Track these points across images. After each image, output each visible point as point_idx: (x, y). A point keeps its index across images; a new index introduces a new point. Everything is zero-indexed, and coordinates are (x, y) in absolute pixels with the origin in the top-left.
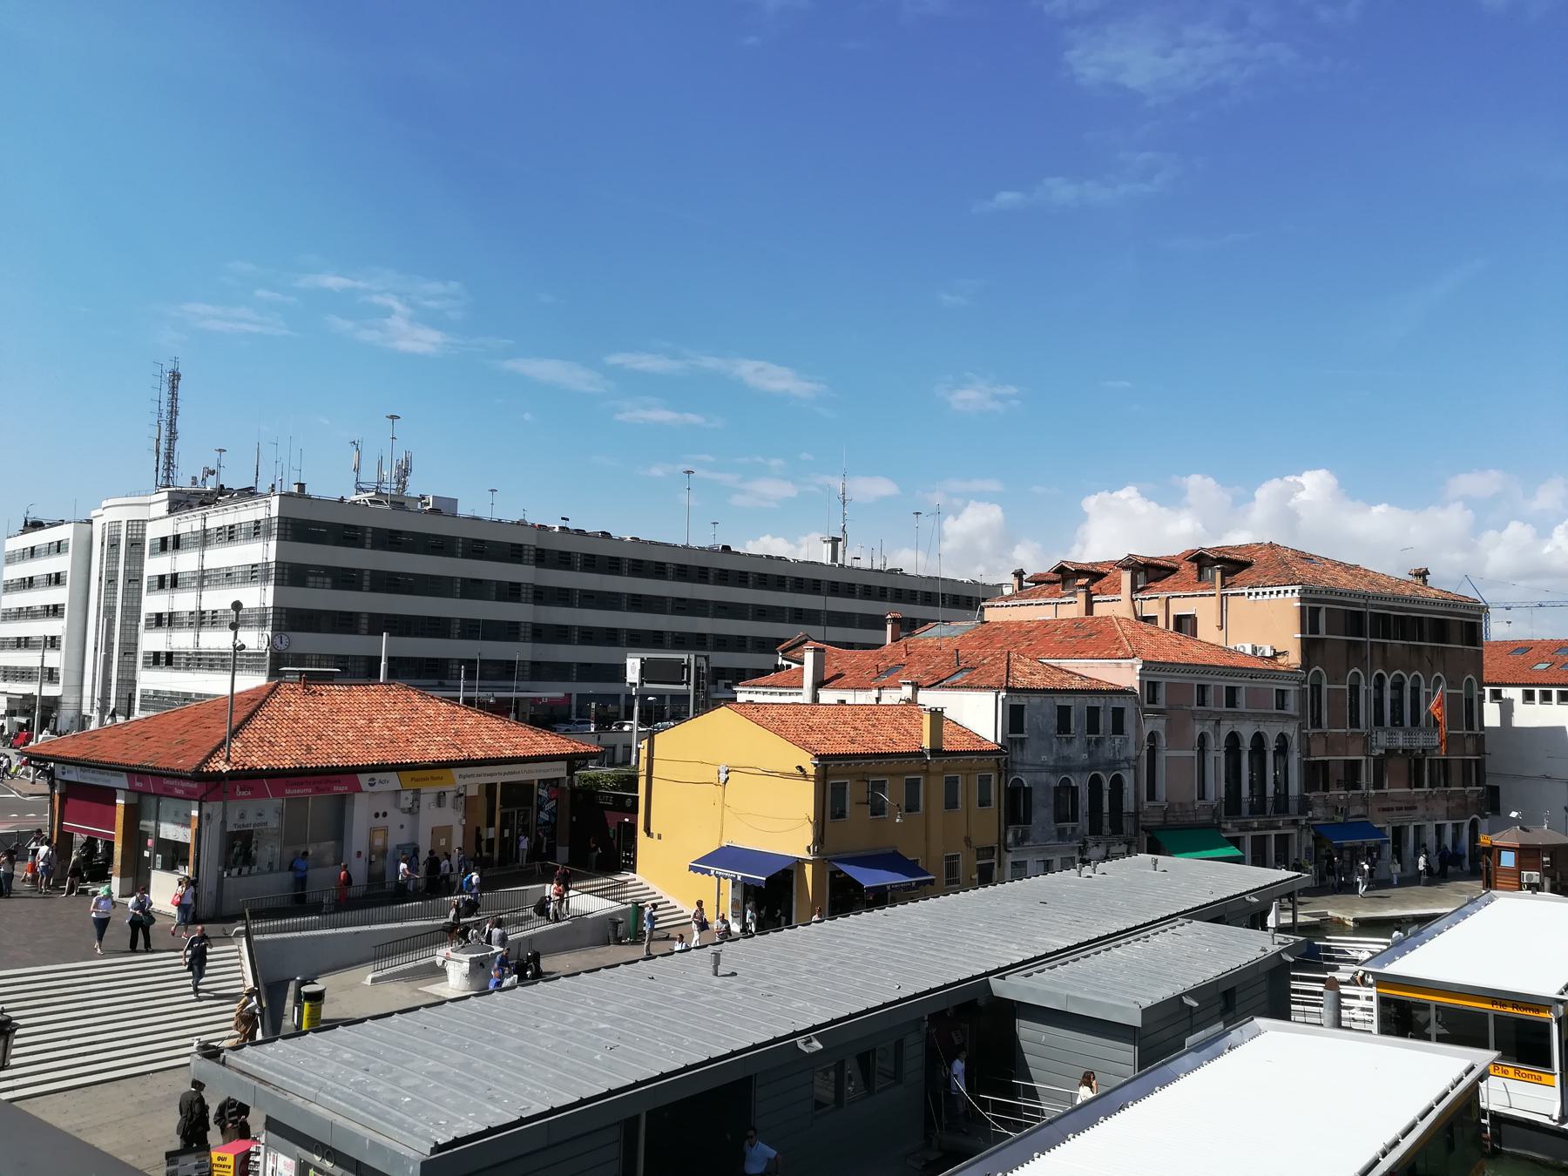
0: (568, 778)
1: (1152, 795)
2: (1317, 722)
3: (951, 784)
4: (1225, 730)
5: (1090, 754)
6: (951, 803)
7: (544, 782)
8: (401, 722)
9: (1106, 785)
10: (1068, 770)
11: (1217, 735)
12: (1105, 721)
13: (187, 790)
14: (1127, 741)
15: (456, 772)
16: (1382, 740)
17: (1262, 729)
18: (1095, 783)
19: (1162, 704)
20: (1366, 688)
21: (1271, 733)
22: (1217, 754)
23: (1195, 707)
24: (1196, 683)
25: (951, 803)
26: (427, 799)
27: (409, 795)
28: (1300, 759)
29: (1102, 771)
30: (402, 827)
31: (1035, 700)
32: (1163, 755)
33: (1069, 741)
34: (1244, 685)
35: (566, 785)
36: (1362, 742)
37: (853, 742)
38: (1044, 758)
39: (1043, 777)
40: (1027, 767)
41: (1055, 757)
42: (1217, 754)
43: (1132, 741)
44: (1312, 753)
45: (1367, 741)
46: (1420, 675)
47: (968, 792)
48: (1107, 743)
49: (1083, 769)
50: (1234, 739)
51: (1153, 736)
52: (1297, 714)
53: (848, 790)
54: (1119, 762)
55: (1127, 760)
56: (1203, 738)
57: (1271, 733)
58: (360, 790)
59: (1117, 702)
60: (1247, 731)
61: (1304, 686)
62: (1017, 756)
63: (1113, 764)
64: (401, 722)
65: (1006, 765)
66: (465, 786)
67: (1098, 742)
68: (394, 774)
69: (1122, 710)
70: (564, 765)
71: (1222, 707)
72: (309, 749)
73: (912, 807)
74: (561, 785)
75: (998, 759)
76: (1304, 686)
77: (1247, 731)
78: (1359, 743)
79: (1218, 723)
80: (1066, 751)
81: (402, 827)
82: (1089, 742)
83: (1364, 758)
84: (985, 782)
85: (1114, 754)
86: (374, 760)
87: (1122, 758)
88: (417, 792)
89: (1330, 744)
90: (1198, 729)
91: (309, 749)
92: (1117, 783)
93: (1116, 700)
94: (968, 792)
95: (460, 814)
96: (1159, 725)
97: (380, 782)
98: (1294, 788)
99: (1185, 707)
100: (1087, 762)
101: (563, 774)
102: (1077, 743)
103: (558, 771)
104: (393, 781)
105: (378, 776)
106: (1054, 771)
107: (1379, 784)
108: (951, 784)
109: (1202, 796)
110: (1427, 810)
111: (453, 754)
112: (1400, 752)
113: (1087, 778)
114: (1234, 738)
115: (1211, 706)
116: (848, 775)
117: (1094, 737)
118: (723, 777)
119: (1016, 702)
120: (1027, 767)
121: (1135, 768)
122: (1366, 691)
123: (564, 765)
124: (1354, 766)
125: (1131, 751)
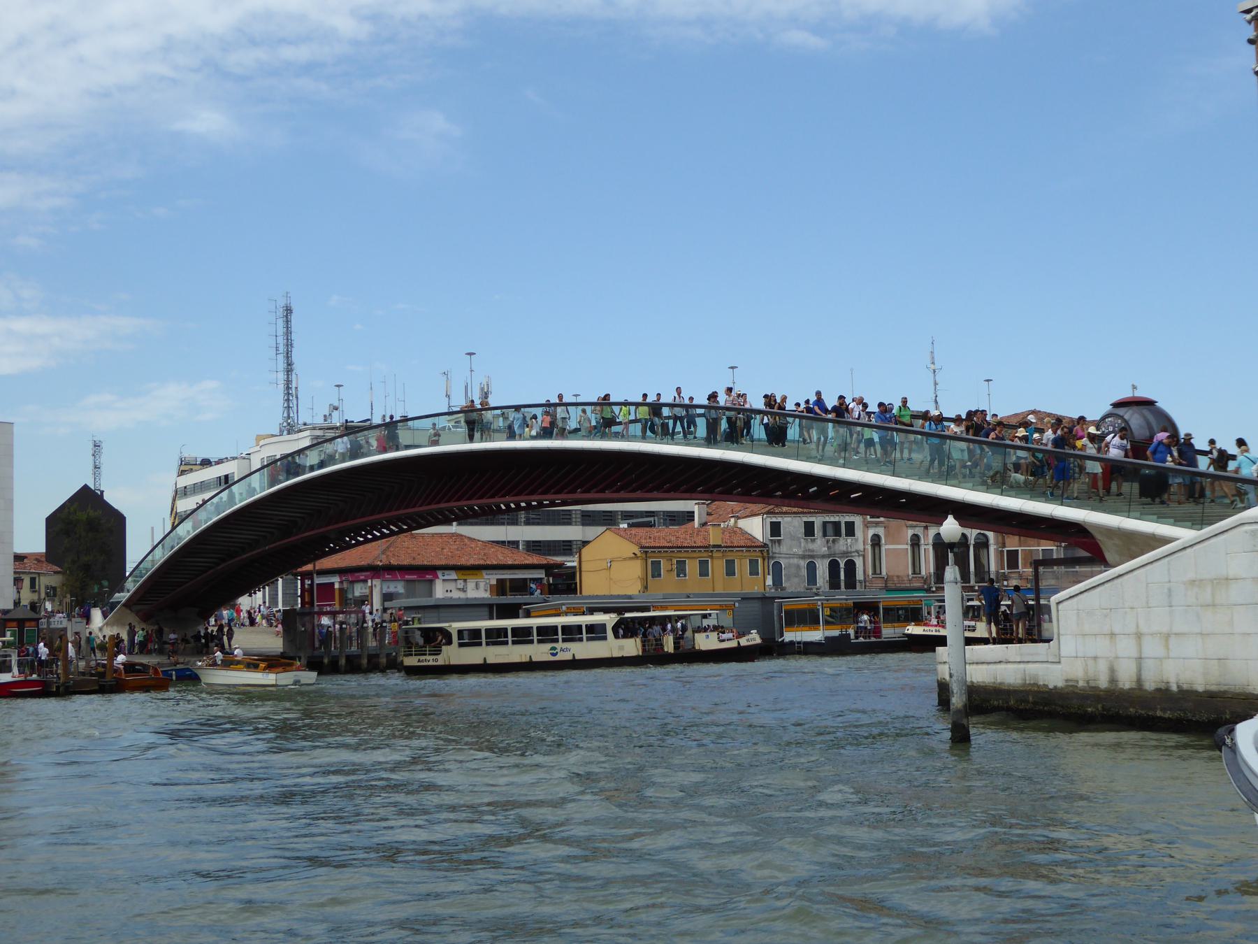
5: (829, 548)
7: (534, 580)
8: (457, 549)
9: (842, 565)
11: (926, 536)
13: (365, 576)
14: (857, 540)
15: (484, 572)
18: (834, 566)
28: (996, 550)
33: (813, 541)
39: (796, 561)
42: (926, 547)
44: (1007, 545)
49: (823, 557)
54: (851, 552)
55: (857, 551)
58: (437, 577)
62: (776, 549)
63: (845, 554)
64: (457, 549)
65: (768, 554)
69: (853, 523)
70: (543, 571)
72: (414, 559)
80: (811, 546)
82: (828, 542)
83: (1055, 548)
85: (847, 548)
86: (443, 563)
87: (853, 550)
91: (414, 559)
92: (851, 566)
101: (543, 576)
104: (453, 575)
105: (446, 572)
106: (803, 557)
111: (481, 562)
113: (827, 562)
116: (663, 557)
119: (774, 520)
121: (864, 556)
123: (543, 571)
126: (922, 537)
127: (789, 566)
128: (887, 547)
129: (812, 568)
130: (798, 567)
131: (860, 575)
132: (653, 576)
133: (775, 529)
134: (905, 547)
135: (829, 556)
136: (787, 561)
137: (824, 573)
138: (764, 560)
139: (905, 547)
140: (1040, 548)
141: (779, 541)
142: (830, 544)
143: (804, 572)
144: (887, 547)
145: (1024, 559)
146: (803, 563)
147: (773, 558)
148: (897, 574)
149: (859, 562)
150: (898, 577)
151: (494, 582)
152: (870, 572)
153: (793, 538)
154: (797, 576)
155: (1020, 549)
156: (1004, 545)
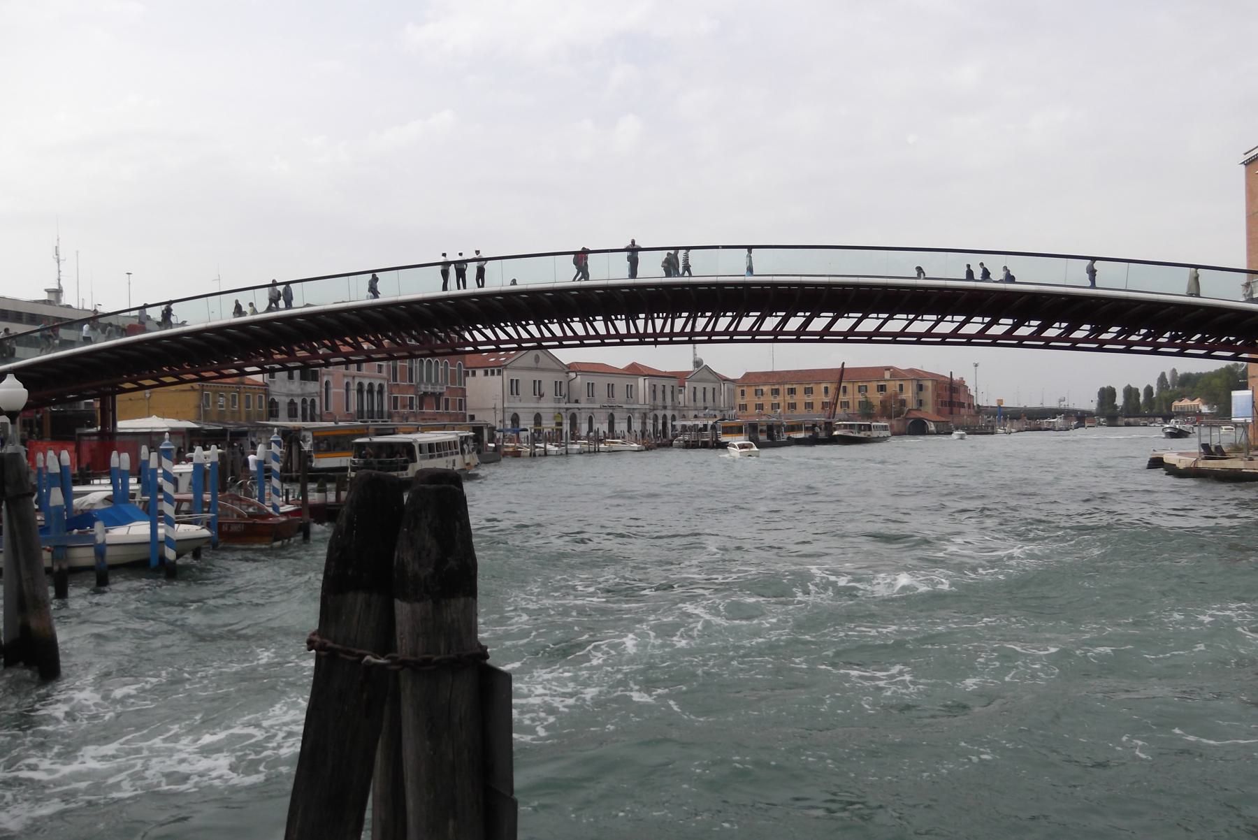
1: (327, 409)
2: (395, 380)
4: (357, 381)
5: (302, 389)
11: (354, 383)
18: (304, 401)
21: (376, 383)
45: (416, 388)
50: (360, 384)
51: (327, 383)
55: (317, 393)
56: (348, 384)
57: (376, 383)
60: (366, 382)
77: (366, 382)
79: (354, 377)
90: (346, 380)
92: (313, 401)
98: (386, 408)
106: (287, 395)
114: (360, 384)
135: (302, 395)
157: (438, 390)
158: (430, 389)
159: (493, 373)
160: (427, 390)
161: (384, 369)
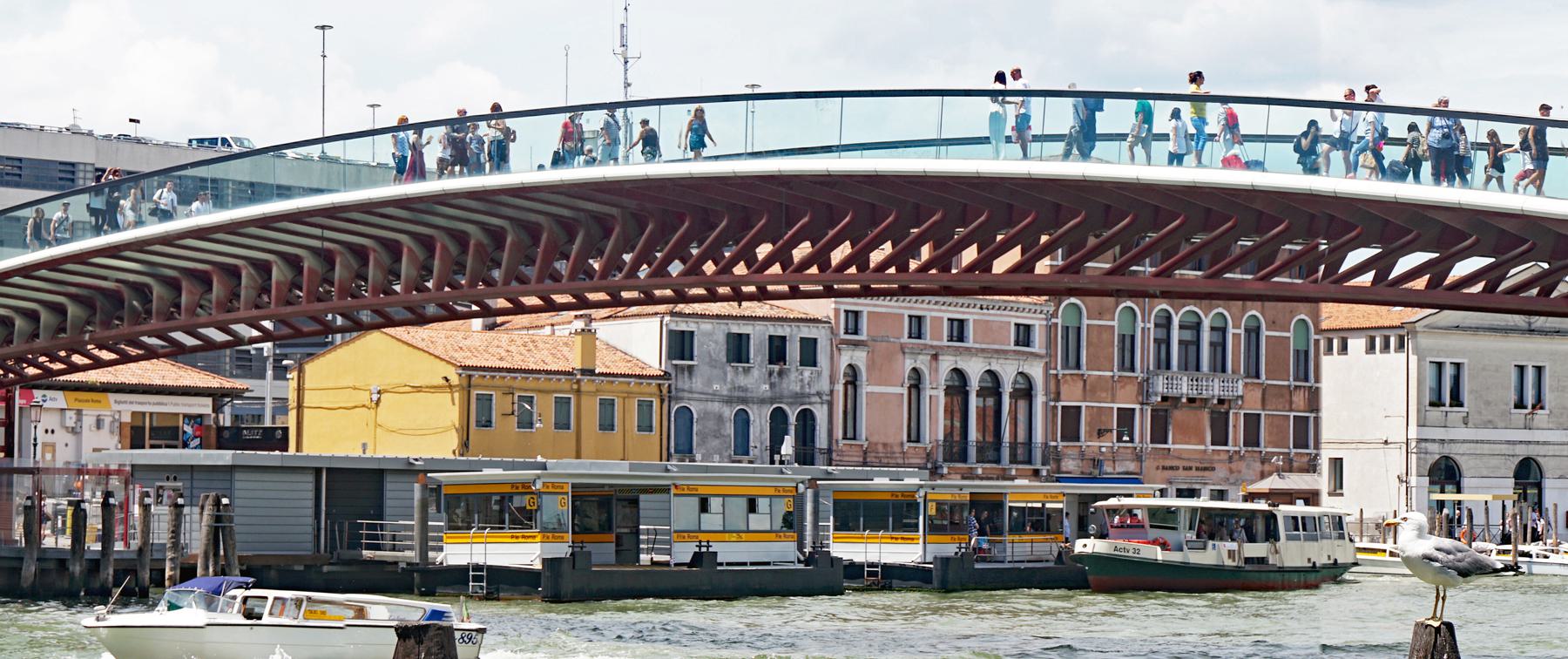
0: (213, 415)
3: (607, 405)
4: (947, 364)
5: (772, 385)
6: (607, 425)
7: (189, 417)
9: (792, 419)
10: (744, 401)
12: (793, 351)
14: (819, 374)
15: (112, 397)
16: (1160, 386)
17: (995, 367)
19: (863, 337)
20: (1145, 328)
22: (934, 393)
23: (905, 339)
24: (907, 313)
25: (607, 425)
26: (89, 421)
27: (71, 415)
28: (1046, 404)
29: (787, 404)
30: (67, 445)
31: (706, 326)
32: (865, 389)
33: (747, 371)
34: (971, 318)
35: (212, 423)
36: (1136, 388)
37: (501, 359)
38: (716, 387)
39: (716, 407)
40: (696, 396)
41: (729, 386)
42: (934, 393)
43: (826, 374)
44: (1062, 396)
45: (1144, 390)
46: (1226, 313)
47: (626, 414)
48: (793, 376)
49: (762, 401)
52: (1043, 352)
53: (494, 402)
54: (809, 395)
55: (819, 394)
57: (1008, 372)
59: (807, 332)
60: (975, 370)
61: (1054, 320)
62: (683, 383)
63: (799, 397)
65: (669, 392)
66: (119, 412)
67: (781, 373)
68: (61, 393)
70: (209, 401)
71: (942, 340)
73: (561, 424)
74: (206, 422)
75: (659, 385)
76: (1054, 320)
77: (975, 370)
78: (1132, 389)
79: (935, 357)
80: (743, 381)
81: (67, 445)
82: (771, 374)
83: (1137, 407)
84: (645, 407)
85: (802, 387)
87: (813, 391)
88: (79, 412)
89: (1089, 390)
90: (909, 364)
92: (807, 418)
93: (806, 329)
94: (626, 414)
95: (116, 438)
96: (860, 358)
97: (51, 399)
98: (1039, 436)
99: (892, 340)
100: (769, 394)
101: (208, 410)
102: (755, 373)
103: (204, 406)
107: (1159, 435)
108: (607, 405)
109: (915, 436)
110: (1231, 471)
112: (1184, 400)
115: (928, 340)
117: (776, 368)
118: (375, 397)
119: (683, 327)
120: (696, 396)
121: (831, 404)
122: (1143, 329)
123: (209, 401)
124: (1126, 417)
125: (824, 385)
126: (926, 372)
127: (705, 415)
128: (870, 389)
129: (743, 421)
130: (720, 418)
131: (821, 441)
132: (479, 424)
133: (680, 345)
134: (898, 390)
136: (702, 406)
137: (762, 432)
138: (662, 401)
139: (898, 390)
140: (1116, 406)
141: (690, 368)
142: (775, 379)
143: (730, 429)
144: (870, 389)
145: (1089, 424)
146: (729, 412)
147: (679, 399)
148: (883, 440)
149: (820, 413)
150: (885, 445)
151: (127, 418)
152: (839, 433)
153: (713, 363)
154: (717, 434)
155: (1083, 404)
156: (1058, 398)
157: (1215, 388)
158: (1184, 387)
159: (1386, 347)
160: (1174, 392)
161: (1038, 337)
